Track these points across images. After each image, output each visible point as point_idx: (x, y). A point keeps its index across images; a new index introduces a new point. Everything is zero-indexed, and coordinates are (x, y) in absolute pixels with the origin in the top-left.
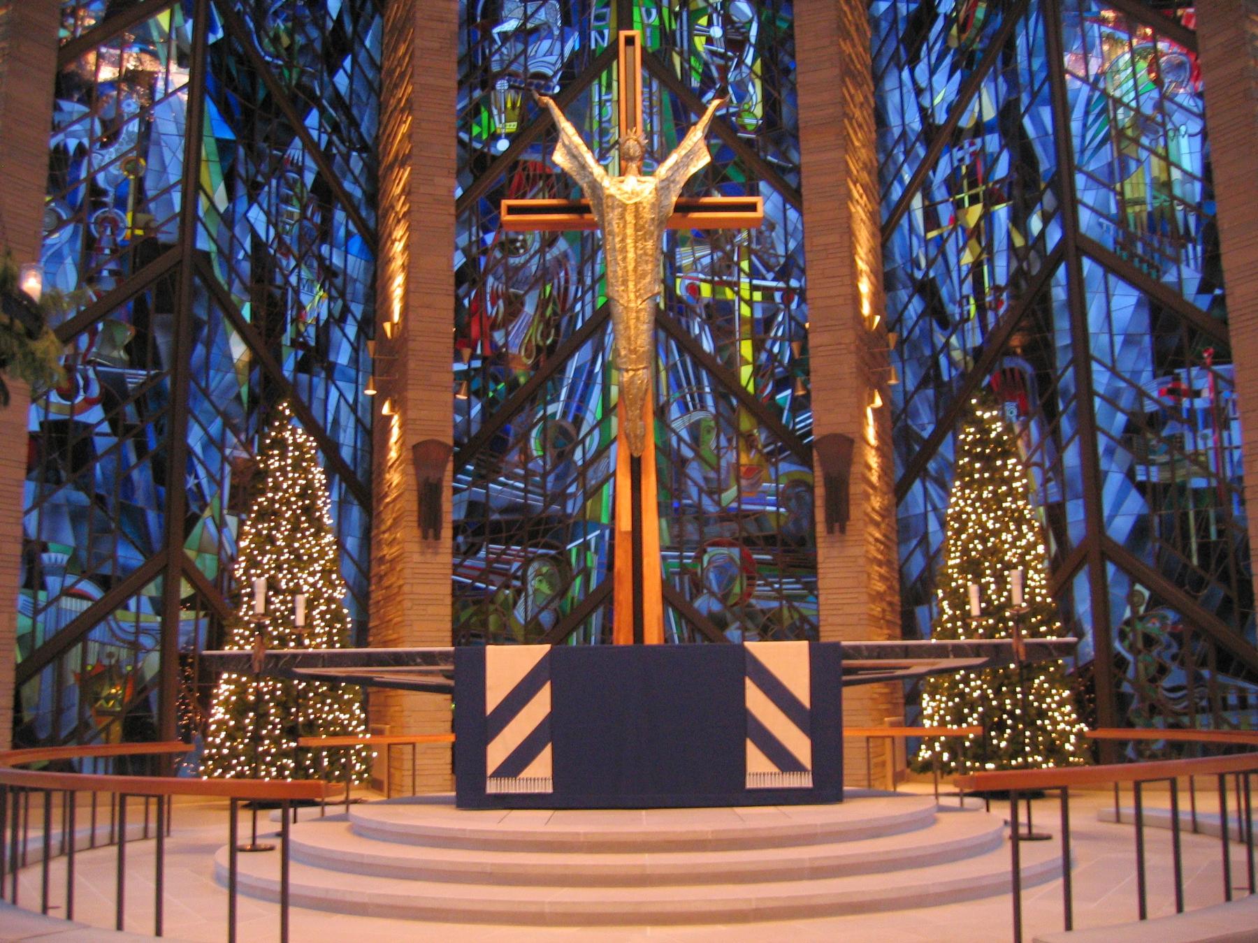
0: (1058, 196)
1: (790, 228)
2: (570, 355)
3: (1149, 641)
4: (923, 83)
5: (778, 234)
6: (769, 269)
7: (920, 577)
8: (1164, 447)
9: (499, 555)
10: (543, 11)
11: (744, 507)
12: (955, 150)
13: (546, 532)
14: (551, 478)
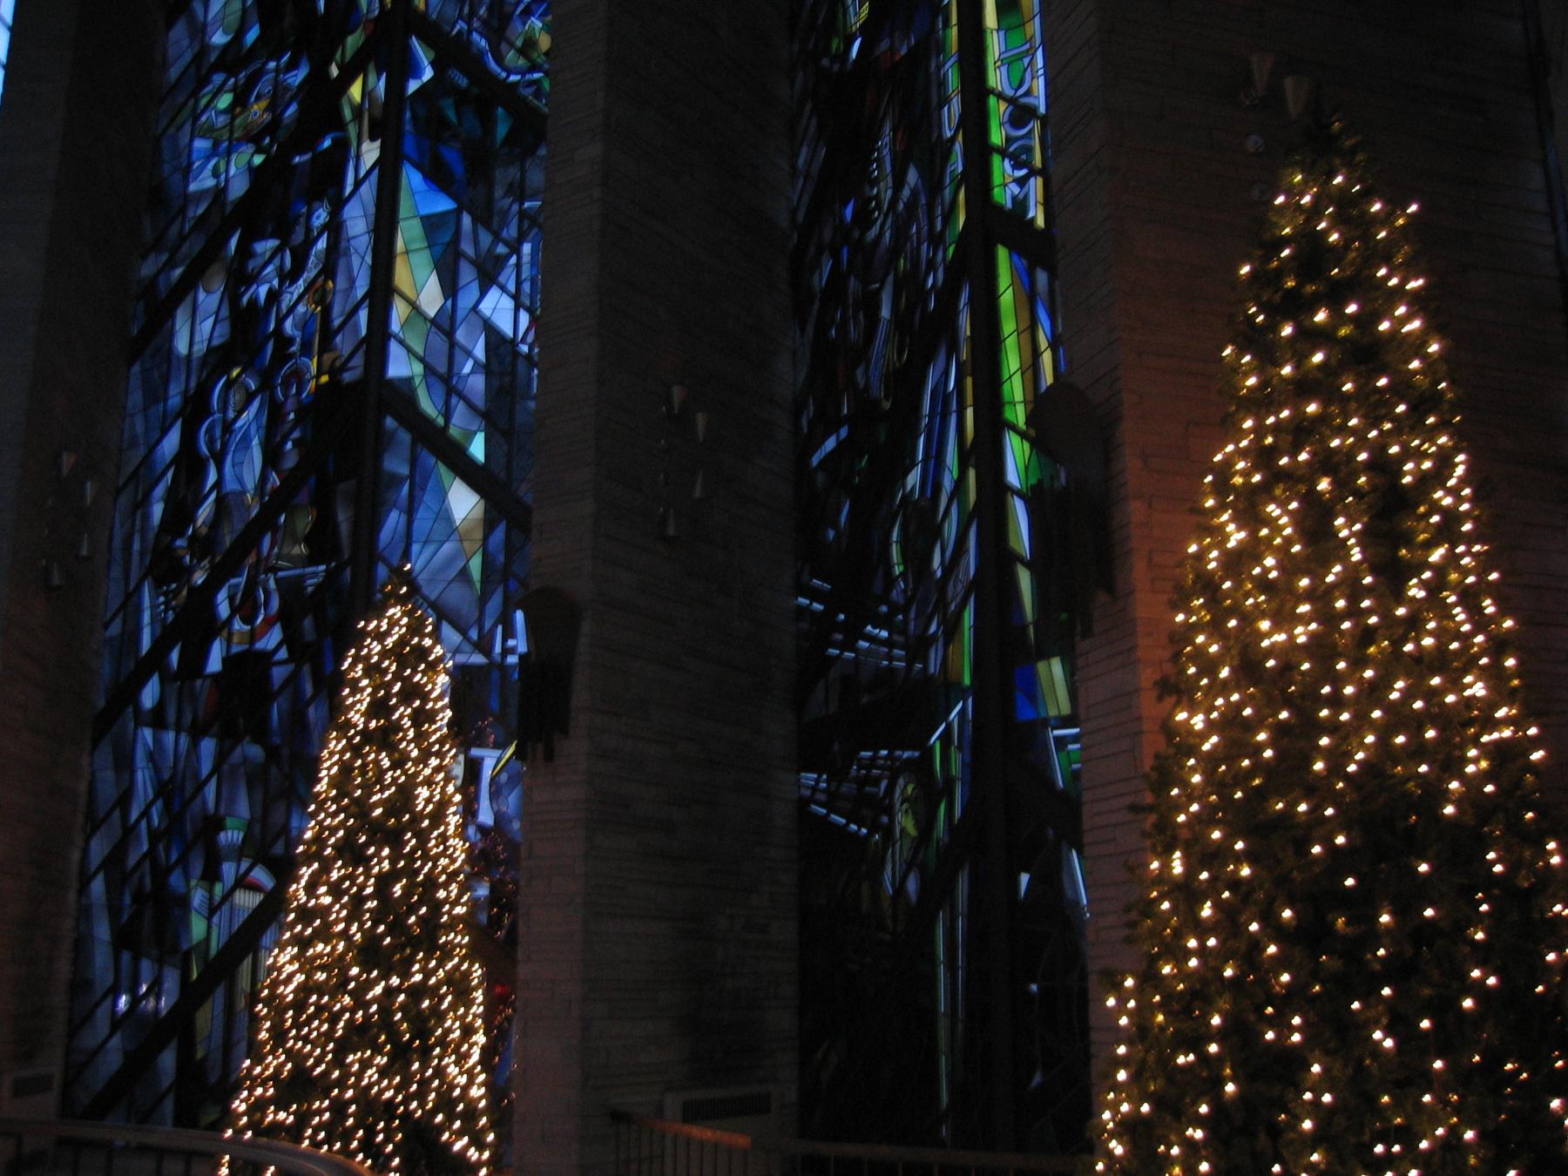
14: (912, 615)
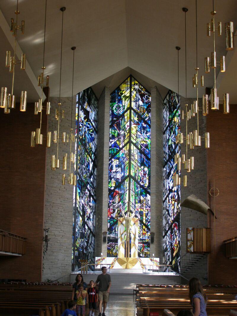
6: (148, 206)
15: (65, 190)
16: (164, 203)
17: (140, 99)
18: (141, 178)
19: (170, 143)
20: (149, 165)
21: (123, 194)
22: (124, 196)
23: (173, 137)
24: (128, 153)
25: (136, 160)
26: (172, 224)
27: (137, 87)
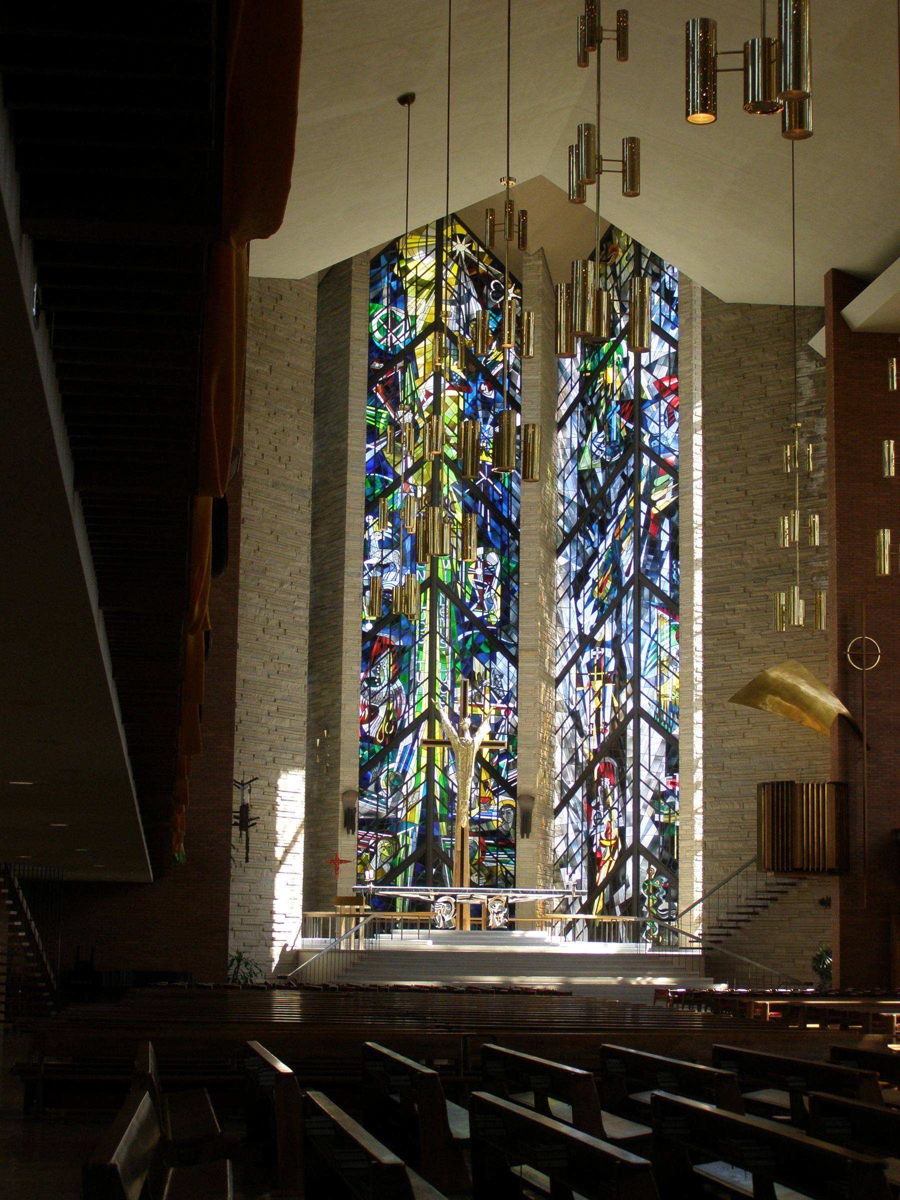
0: (633, 687)
1: (510, 677)
2: (402, 740)
3: (655, 890)
4: (581, 611)
5: (504, 680)
6: (499, 698)
7: (563, 855)
8: (667, 807)
9: (363, 836)
10: (391, 555)
11: (481, 817)
12: (592, 650)
13: (387, 826)
14: (390, 800)
15: (281, 631)
16: (556, 687)
17: (474, 293)
18: (473, 590)
19: (586, 462)
20: (502, 543)
21: (409, 650)
22: (413, 657)
23: (601, 440)
24: (430, 494)
25: (458, 522)
26: (591, 764)
27: (461, 248)
